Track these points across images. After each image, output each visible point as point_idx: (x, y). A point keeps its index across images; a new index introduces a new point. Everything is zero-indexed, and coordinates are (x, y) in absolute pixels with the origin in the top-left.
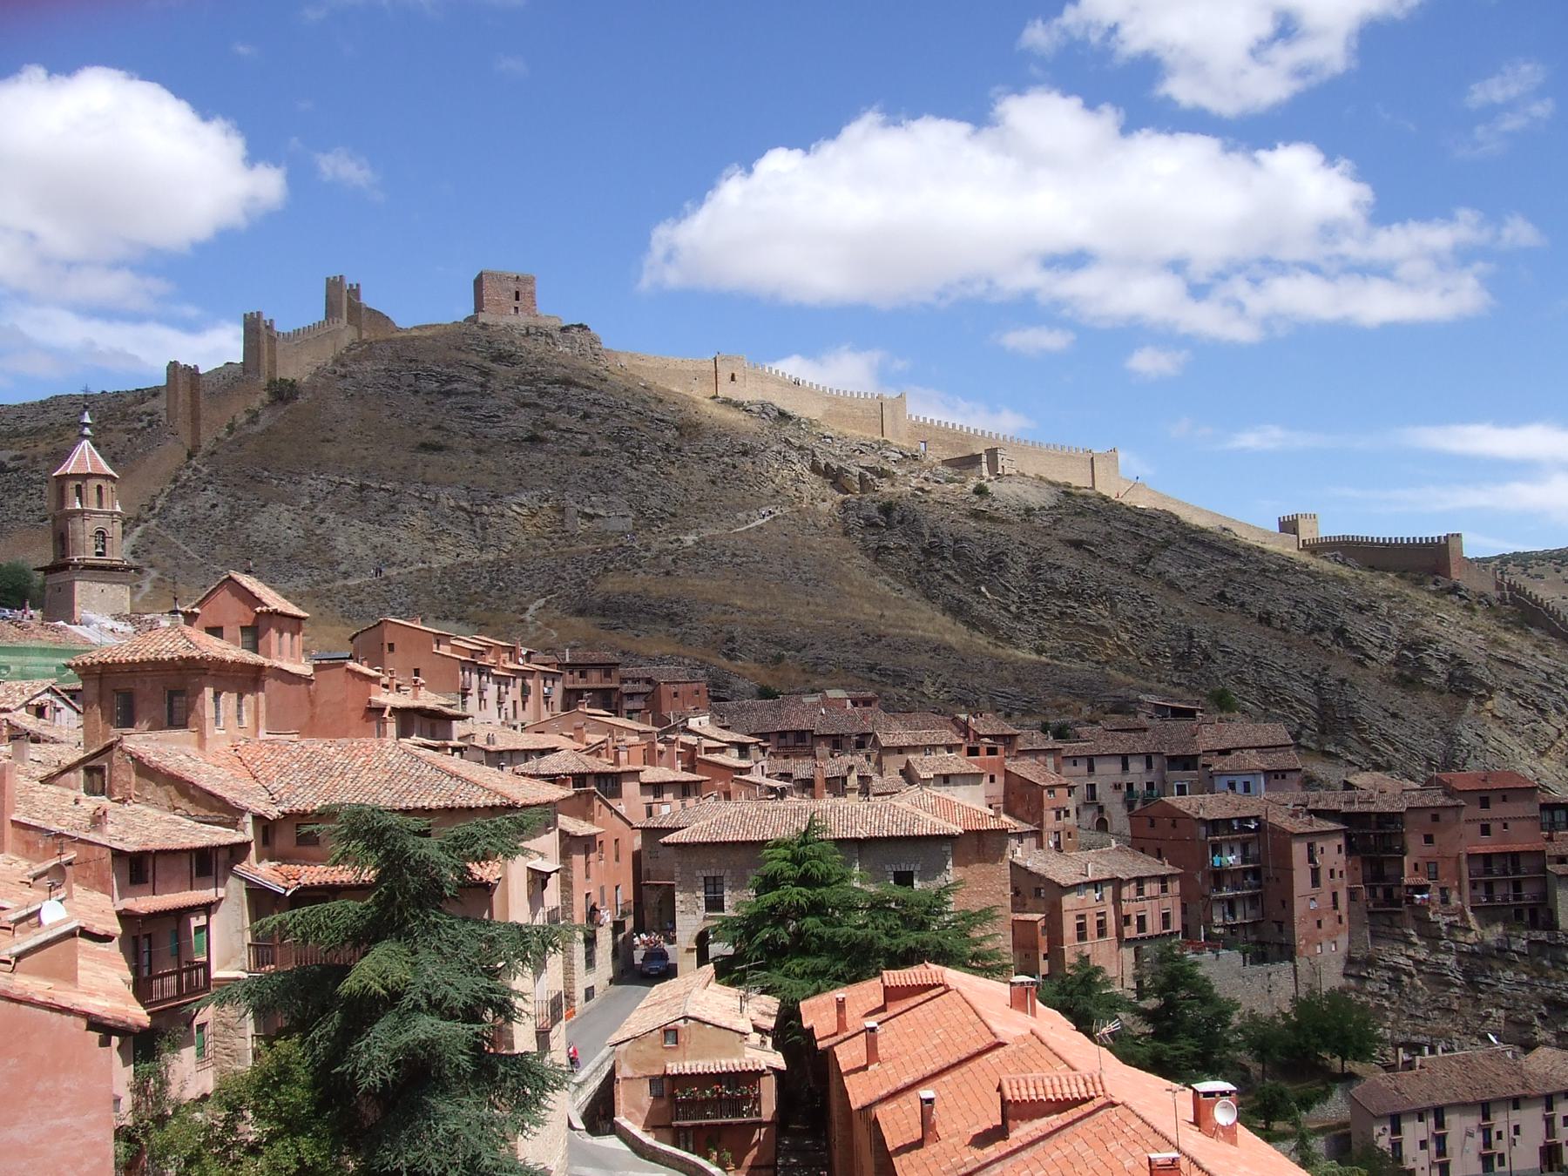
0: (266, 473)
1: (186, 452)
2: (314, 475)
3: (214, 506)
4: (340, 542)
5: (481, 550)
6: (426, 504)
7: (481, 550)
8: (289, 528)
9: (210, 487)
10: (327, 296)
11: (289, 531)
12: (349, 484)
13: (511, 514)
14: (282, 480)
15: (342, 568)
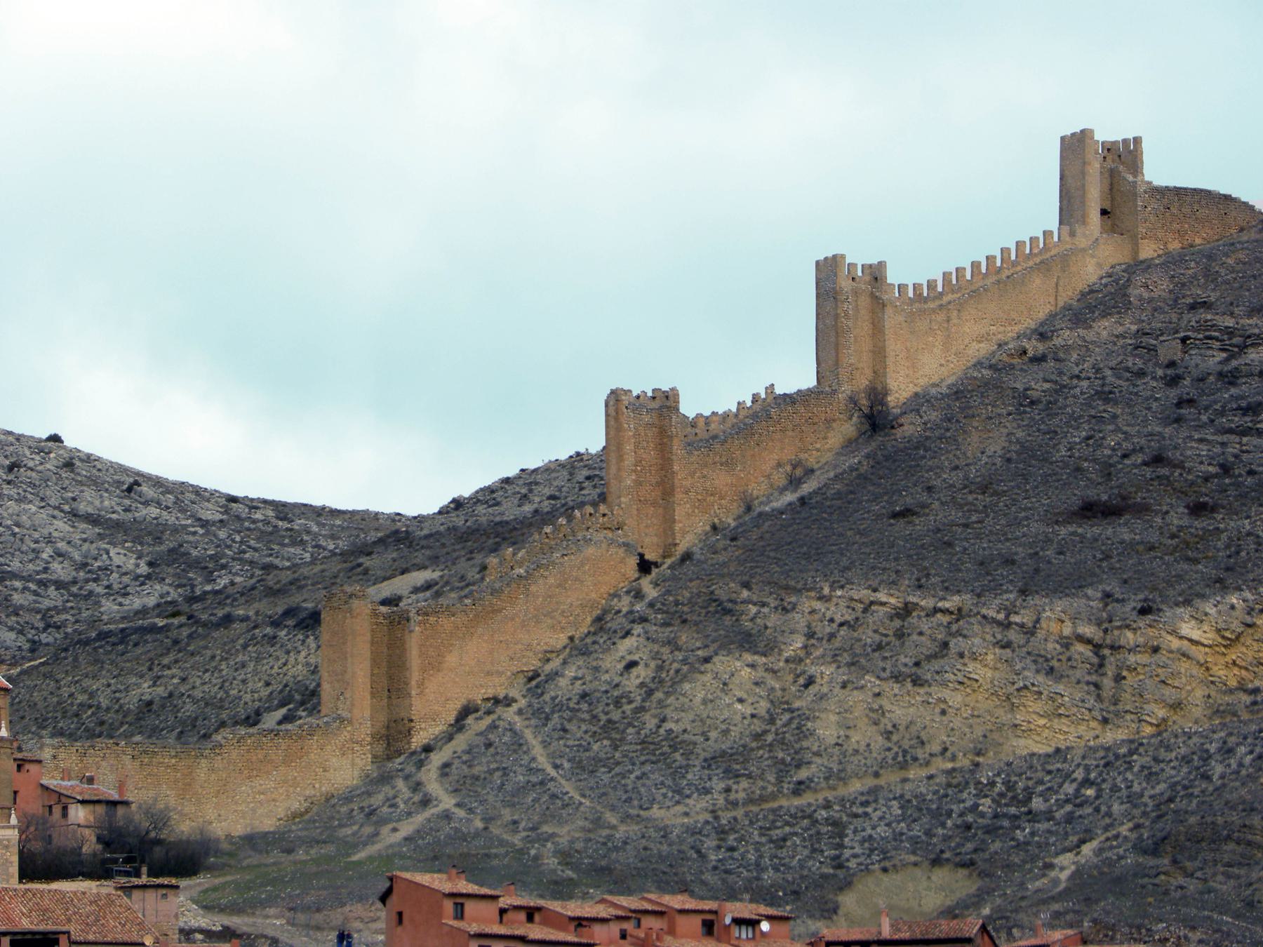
0: (745, 594)
1: (633, 561)
2: (826, 591)
3: (632, 665)
4: (826, 729)
5: (1105, 721)
6: (1013, 635)
7: (1105, 721)
8: (741, 701)
9: (638, 629)
10: (1061, 179)
11: (739, 706)
12: (883, 604)
13: (1176, 644)
14: (764, 605)
15: (803, 774)
